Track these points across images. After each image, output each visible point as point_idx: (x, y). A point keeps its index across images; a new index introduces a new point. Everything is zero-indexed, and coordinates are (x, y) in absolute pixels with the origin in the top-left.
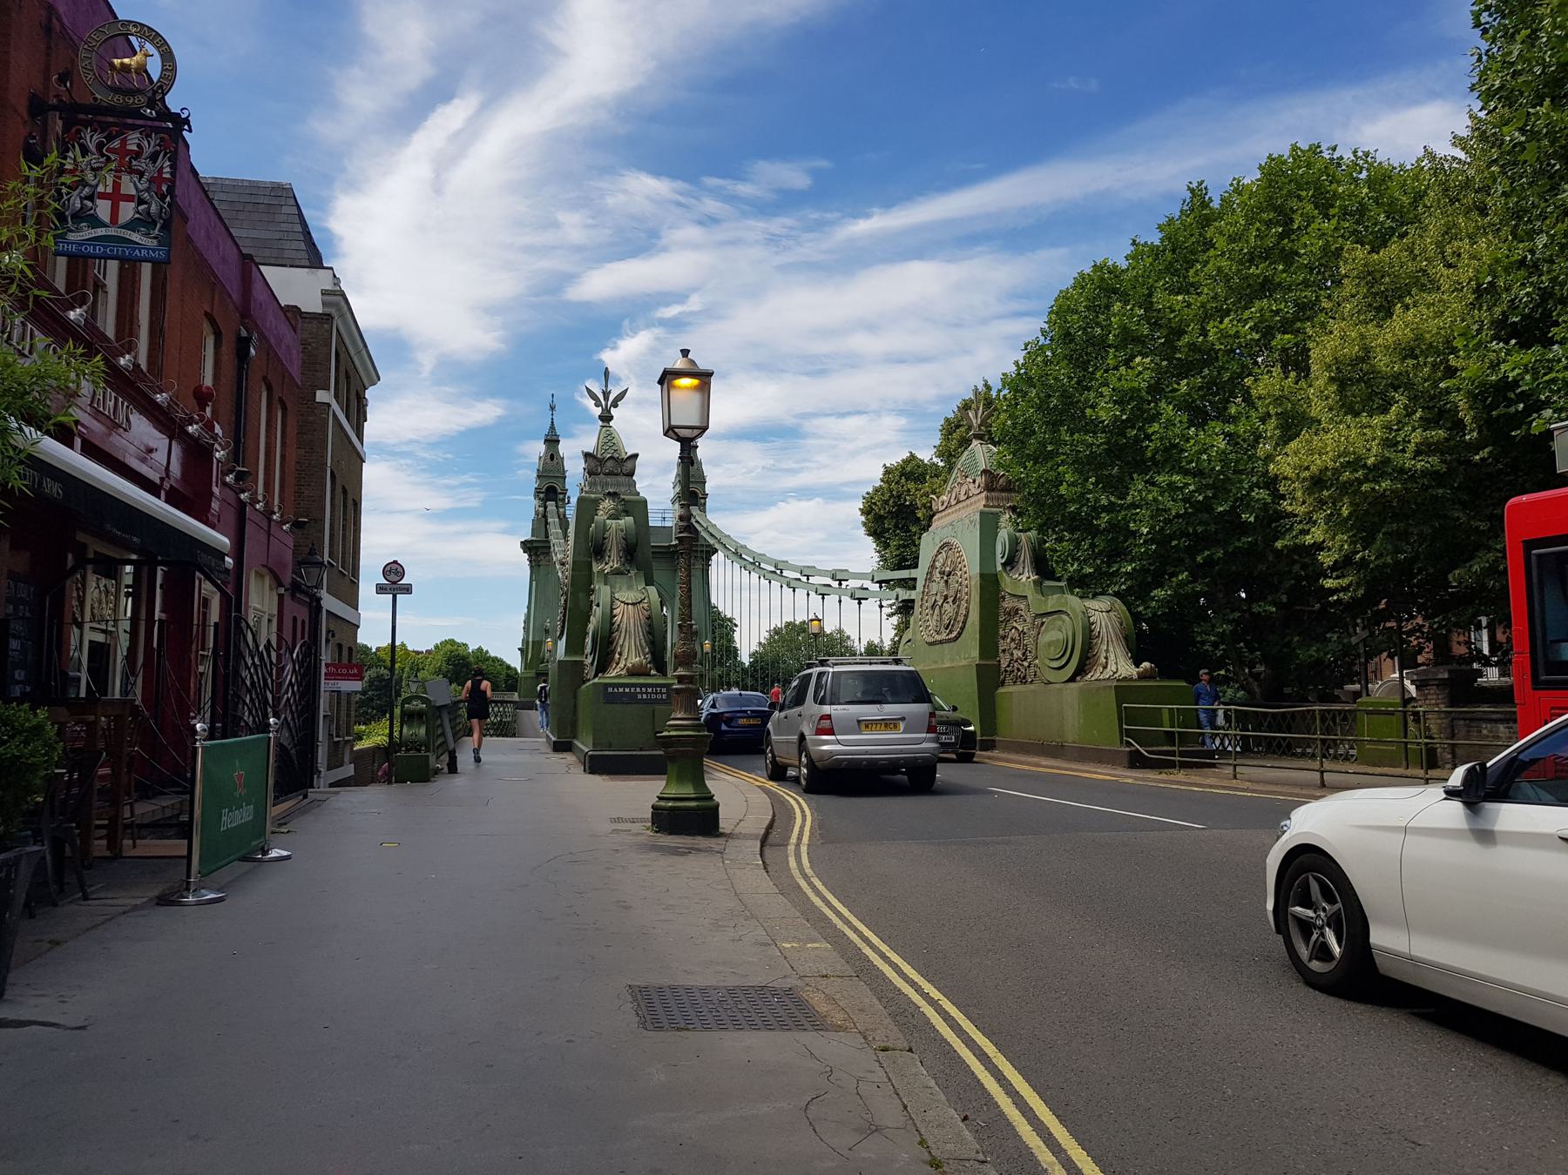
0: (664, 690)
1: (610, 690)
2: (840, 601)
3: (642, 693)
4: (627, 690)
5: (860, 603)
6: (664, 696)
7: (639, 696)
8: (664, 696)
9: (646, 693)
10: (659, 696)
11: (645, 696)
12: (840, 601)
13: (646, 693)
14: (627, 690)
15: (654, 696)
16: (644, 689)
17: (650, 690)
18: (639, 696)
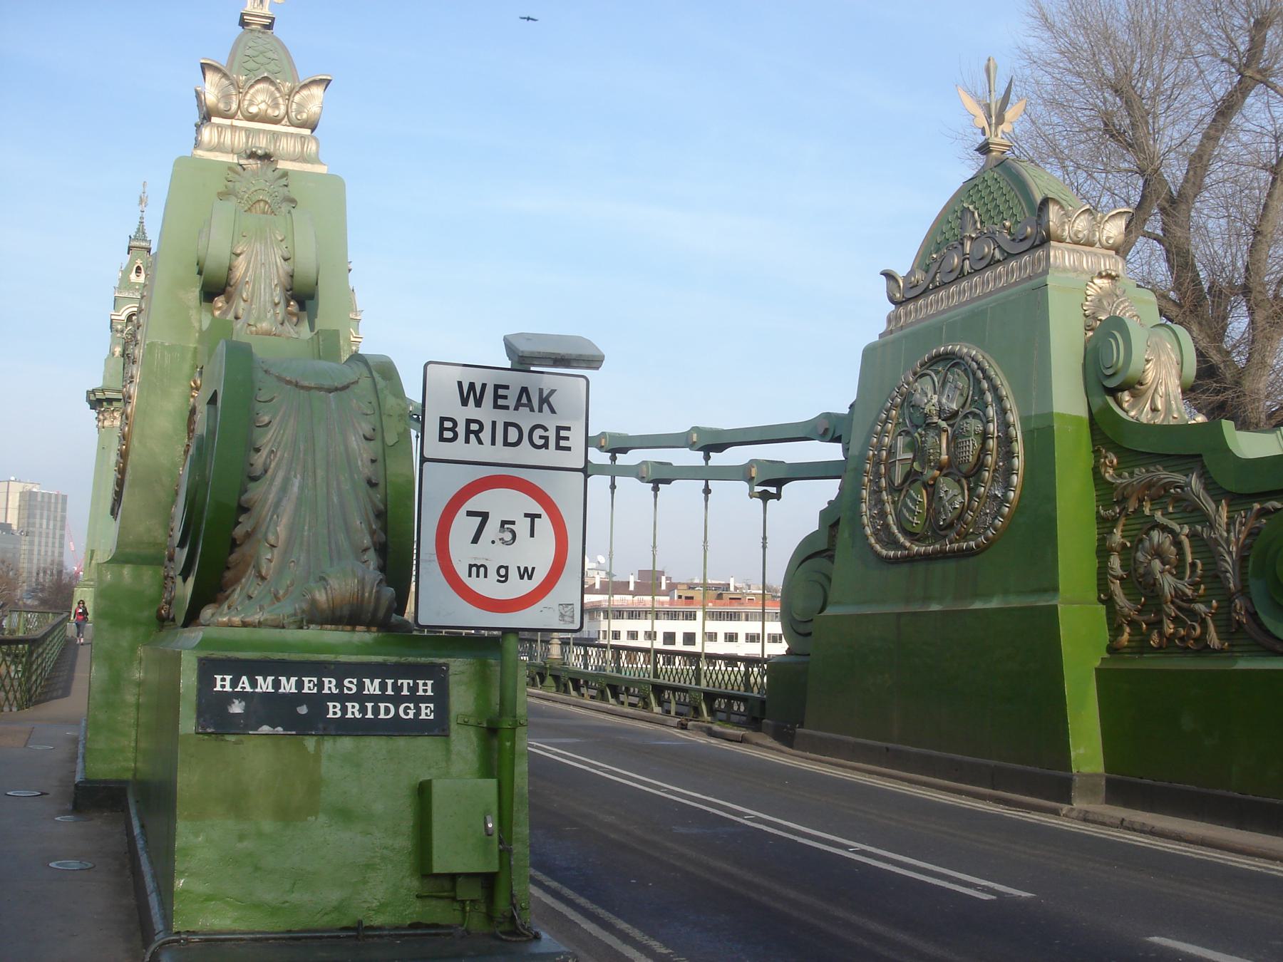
0: (426, 687)
1: (223, 683)
2: (613, 487)
3: (342, 698)
4: (288, 686)
5: (656, 489)
6: (427, 712)
7: (334, 710)
8: (427, 712)
9: (360, 698)
10: (407, 712)
11: (353, 710)
12: (613, 487)
13: (360, 698)
14: (288, 686)
15: (386, 712)
16: (350, 685)
17: (372, 687)
18: (334, 710)
